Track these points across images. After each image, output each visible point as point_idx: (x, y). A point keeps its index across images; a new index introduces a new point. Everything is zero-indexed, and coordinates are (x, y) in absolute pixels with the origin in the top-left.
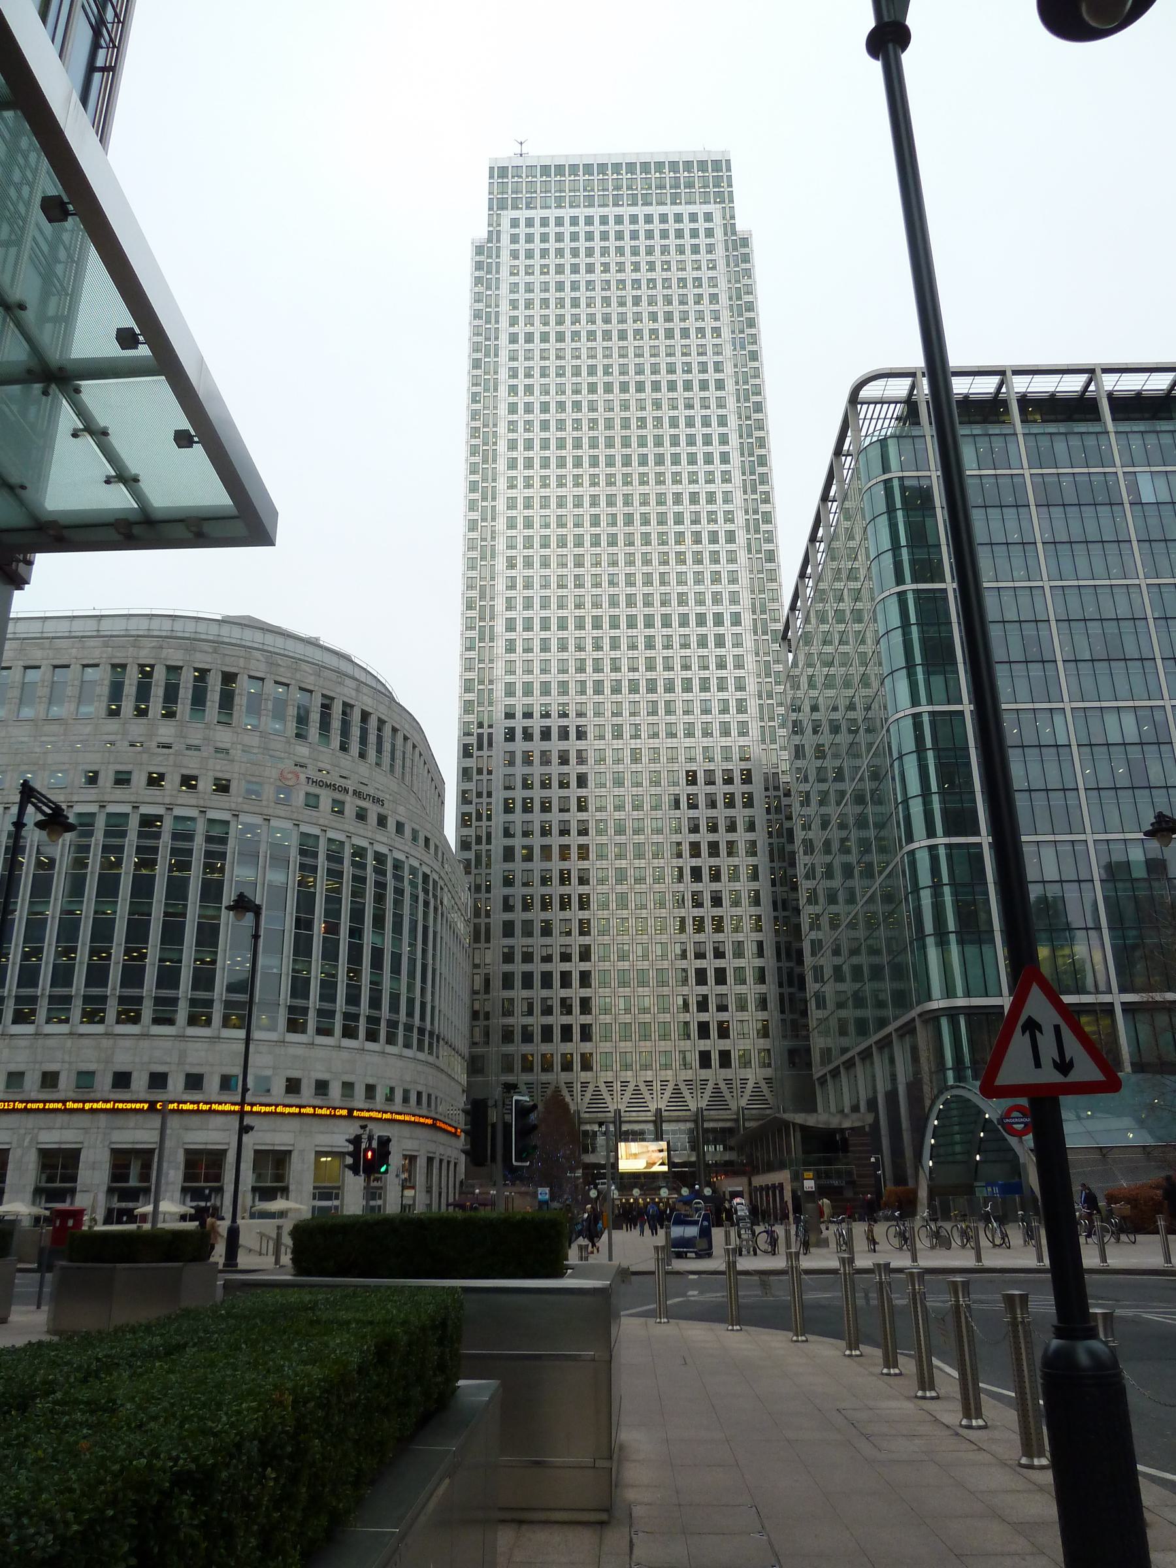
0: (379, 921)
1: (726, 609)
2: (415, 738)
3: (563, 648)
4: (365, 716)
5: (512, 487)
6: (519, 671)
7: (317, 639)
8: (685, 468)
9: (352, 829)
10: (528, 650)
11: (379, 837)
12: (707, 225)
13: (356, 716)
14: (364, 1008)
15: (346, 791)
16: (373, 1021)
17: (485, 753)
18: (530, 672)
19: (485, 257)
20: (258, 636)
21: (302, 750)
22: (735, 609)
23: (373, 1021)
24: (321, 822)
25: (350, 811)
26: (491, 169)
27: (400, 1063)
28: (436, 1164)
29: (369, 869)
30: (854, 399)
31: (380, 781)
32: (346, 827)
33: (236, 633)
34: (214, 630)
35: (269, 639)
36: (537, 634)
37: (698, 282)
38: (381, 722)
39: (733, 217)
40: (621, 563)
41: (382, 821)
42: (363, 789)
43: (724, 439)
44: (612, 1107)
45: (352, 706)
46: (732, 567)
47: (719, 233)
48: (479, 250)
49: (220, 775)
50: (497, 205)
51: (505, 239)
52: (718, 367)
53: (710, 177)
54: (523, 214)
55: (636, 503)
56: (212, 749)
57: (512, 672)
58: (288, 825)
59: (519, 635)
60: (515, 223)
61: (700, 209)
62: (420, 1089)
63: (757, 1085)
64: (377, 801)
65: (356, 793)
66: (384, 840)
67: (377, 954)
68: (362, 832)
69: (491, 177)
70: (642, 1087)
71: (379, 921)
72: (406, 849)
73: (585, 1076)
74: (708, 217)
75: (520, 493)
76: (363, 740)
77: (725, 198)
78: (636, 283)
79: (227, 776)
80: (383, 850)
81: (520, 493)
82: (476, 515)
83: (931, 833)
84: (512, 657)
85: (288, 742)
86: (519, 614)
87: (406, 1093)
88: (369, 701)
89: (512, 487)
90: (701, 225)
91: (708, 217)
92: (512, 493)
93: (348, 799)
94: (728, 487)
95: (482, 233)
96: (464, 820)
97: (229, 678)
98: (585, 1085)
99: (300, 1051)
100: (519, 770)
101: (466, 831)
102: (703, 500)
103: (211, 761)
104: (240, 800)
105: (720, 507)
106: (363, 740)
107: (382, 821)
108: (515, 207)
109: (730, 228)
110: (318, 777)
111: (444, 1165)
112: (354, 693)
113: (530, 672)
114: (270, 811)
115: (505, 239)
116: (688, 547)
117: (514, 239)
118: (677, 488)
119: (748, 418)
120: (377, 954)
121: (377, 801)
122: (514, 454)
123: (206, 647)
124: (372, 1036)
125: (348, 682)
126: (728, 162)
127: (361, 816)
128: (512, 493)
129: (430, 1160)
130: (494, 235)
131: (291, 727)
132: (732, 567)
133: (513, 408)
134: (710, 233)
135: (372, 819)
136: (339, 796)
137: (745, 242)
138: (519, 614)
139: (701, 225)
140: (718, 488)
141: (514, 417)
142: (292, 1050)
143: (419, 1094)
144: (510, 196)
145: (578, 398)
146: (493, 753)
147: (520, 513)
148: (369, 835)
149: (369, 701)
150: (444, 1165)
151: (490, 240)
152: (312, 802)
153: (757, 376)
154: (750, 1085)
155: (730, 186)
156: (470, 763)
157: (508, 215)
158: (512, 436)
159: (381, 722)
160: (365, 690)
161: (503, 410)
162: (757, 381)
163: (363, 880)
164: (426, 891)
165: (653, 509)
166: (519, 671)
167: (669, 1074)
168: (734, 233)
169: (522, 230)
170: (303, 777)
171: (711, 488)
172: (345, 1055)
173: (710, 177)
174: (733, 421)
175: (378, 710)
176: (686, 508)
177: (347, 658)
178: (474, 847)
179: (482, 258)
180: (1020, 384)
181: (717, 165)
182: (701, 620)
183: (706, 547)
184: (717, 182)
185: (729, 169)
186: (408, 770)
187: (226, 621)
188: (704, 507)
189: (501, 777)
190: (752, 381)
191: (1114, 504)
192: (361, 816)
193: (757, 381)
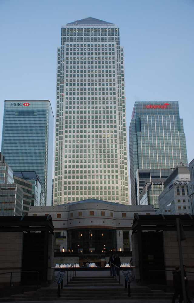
19: (60, 51)
26: (62, 29)
39: (119, 44)
47: (116, 50)
48: (59, 50)
51: (65, 50)
54: (70, 43)
60: (68, 45)
61: (111, 43)
90: (111, 47)
91: (113, 45)
92: (67, 115)
95: (60, 45)
126: (119, 29)
130: (62, 48)
151: (62, 49)
173: (114, 34)
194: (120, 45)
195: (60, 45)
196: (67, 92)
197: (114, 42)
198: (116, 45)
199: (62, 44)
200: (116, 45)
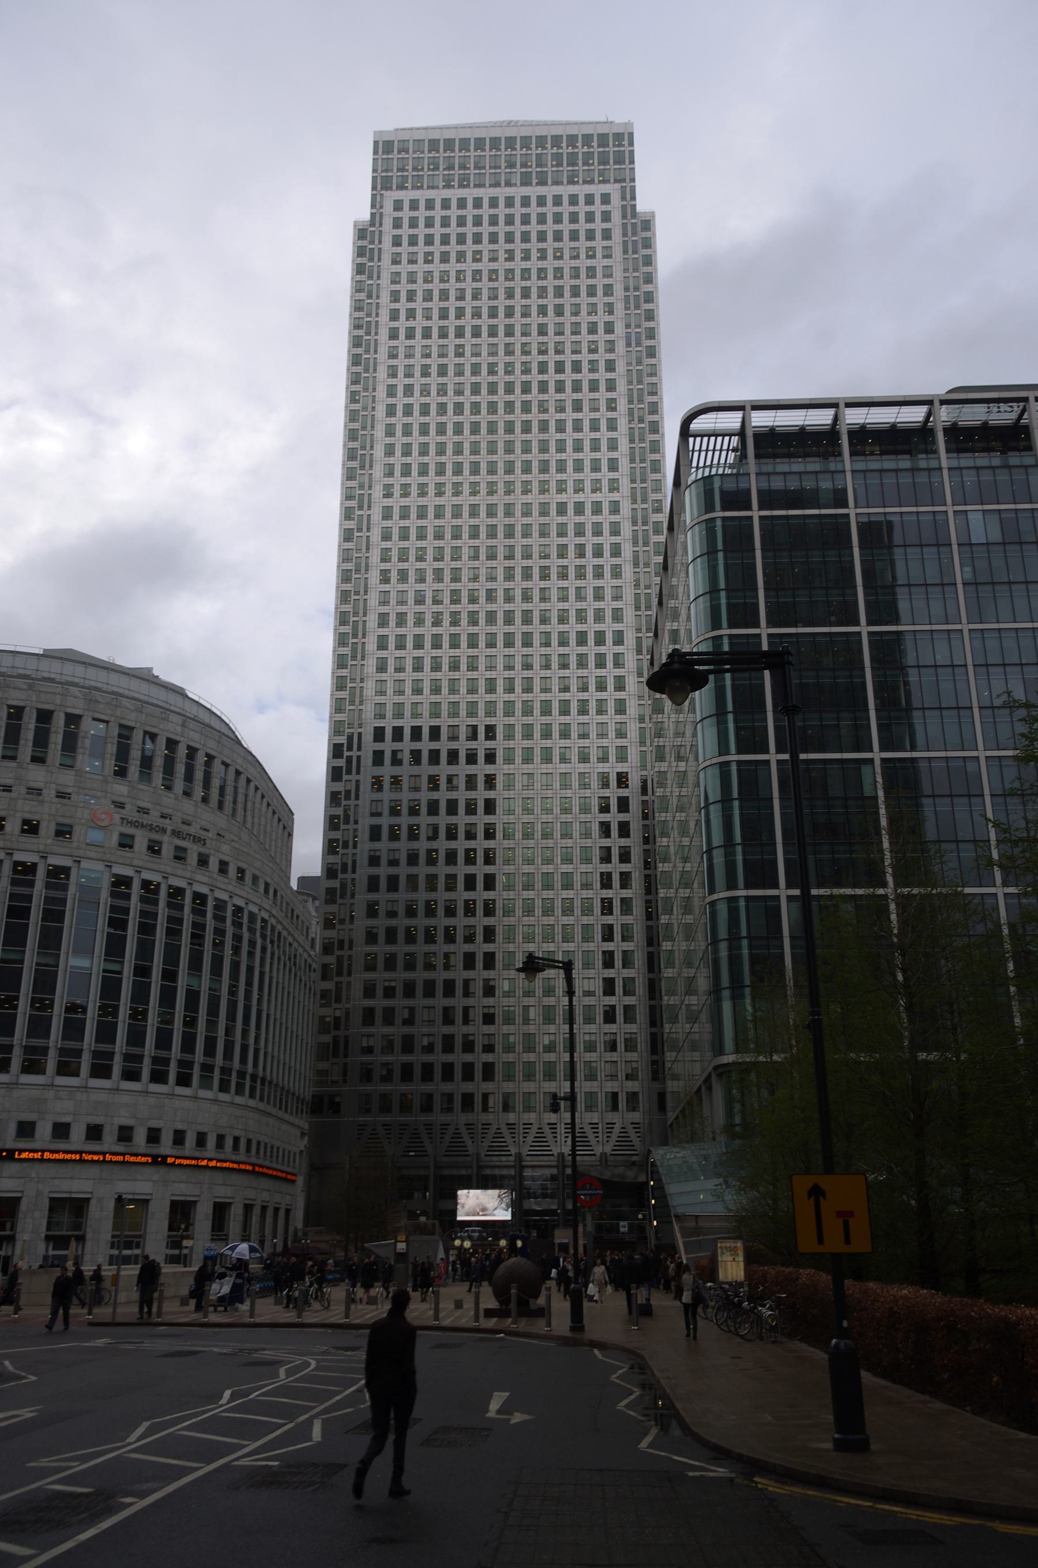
0: (195, 964)
1: (609, 627)
2: (252, 772)
3: (436, 667)
4: (192, 752)
5: (388, 495)
6: (390, 692)
7: (150, 670)
8: (570, 476)
9: (169, 870)
10: (399, 669)
11: (199, 877)
12: (604, 208)
13: (182, 752)
14: (176, 1051)
15: (164, 831)
16: (185, 1065)
18: (401, 693)
20: (80, 670)
21: (120, 789)
22: (618, 627)
23: (185, 1065)
24: (136, 862)
25: (167, 851)
26: (376, 143)
27: (215, 1108)
28: (256, 1211)
29: (187, 910)
30: (685, 432)
31: (208, 818)
32: (163, 868)
33: (53, 669)
34: (32, 664)
35: (92, 673)
36: (410, 653)
37: (591, 272)
38: (210, 758)
39: (633, 198)
41: (203, 861)
42: (185, 829)
43: (613, 446)
44: (471, 1149)
45: (176, 743)
49: (28, 816)
50: (381, 184)
51: (388, 223)
52: (610, 366)
53: (608, 152)
54: (406, 196)
55: (518, 513)
56: (24, 791)
57: (382, 693)
58: (100, 866)
59: (391, 654)
60: (398, 206)
61: (597, 190)
62: (237, 1133)
63: (624, 1130)
64: (197, 840)
65: (177, 834)
66: (205, 879)
67: (193, 997)
68: (180, 872)
69: (375, 152)
70: (505, 1130)
71: (195, 964)
72: (230, 888)
73: (443, 1118)
75: (396, 502)
76: (189, 777)
78: (526, 274)
79: (37, 817)
80: (204, 890)
81: (396, 502)
82: (351, 525)
83: (732, 885)
84: (383, 676)
85: (106, 781)
86: (391, 631)
87: (221, 1138)
88: (196, 736)
89: (388, 495)
91: (606, 199)
92: (388, 502)
93: (166, 839)
94: (615, 496)
95: (365, 214)
97: (45, 716)
98: (445, 1126)
99: (103, 1097)
100: (387, 795)
101: (333, 859)
102: (588, 511)
103: (20, 802)
104: (49, 841)
105: (606, 518)
106: (189, 777)
107: (203, 861)
108: (401, 187)
109: (629, 210)
110: (136, 816)
111: (270, 1213)
112: (179, 729)
113: (401, 693)
114: (81, 853)
115: (388, 223)
116: (571, 561)
117: (397, 224)
118: (562, 498)
119: (641, 420)
120: (193, 997)
121: (197, 840)
123: (20, 683)
124: (184, 1080)
125: (173, 718)
126: (631, 135)
127: (180, 855)
128: (388, 502)
129: (248, 1208)
130: (376, 218)
131: (110, 765)
133: (391, 411)
134: (606, 217)
135: (193, 859)
136: (156, 836)
137: (647, 224)
138: (391, 631)
139: (598, 208)
140: (605, 497)
142: (95, 1096)
143: (236, 1139)
144: (394, 173)
145: (461, 399)
146: (360, 777)
147: (395, 524)
148: (188, 875)
149: (196, 736)
150: (270, 1213)
151: (372, 223)
152: (126, 843)
153: (653, 374)
154: (617, 1129)
155: (632, 162)
157: (391, 196)
159: (210, 758)
160: (191, 724)
161: (380, 412)
162: (654, 380)
163: (180, 922)
164: (252, 930)
165: (535, 520)
166: (390, 692)
167: (532, 1117)
168: (634, 214)
169: (406, 214)
170: (117, 818)
172: (152, 1100)
173: (608, 152)
174: (623, 425)
175: (206, 745)
176: (571, 519)
177: (180, 692)
178: (340, 876)
179: (364, 243)
180: (854, 417)
181: (619, 137)
182: (582, 639)
183: (590, 561)
184: (619, 160)
185: (631, 143)
186: (240, 806)
187: (49, 655)
188: (589, 519)
189: (368, 803)
190: (648, 380)
191: (942, 544)
192: (180, 855)
193: (654, 380)
194: (640, 208)
195: (367, 217)
196: (391, 401)
197: (613, 189)
199: (373, 206)
200: (616, 200)
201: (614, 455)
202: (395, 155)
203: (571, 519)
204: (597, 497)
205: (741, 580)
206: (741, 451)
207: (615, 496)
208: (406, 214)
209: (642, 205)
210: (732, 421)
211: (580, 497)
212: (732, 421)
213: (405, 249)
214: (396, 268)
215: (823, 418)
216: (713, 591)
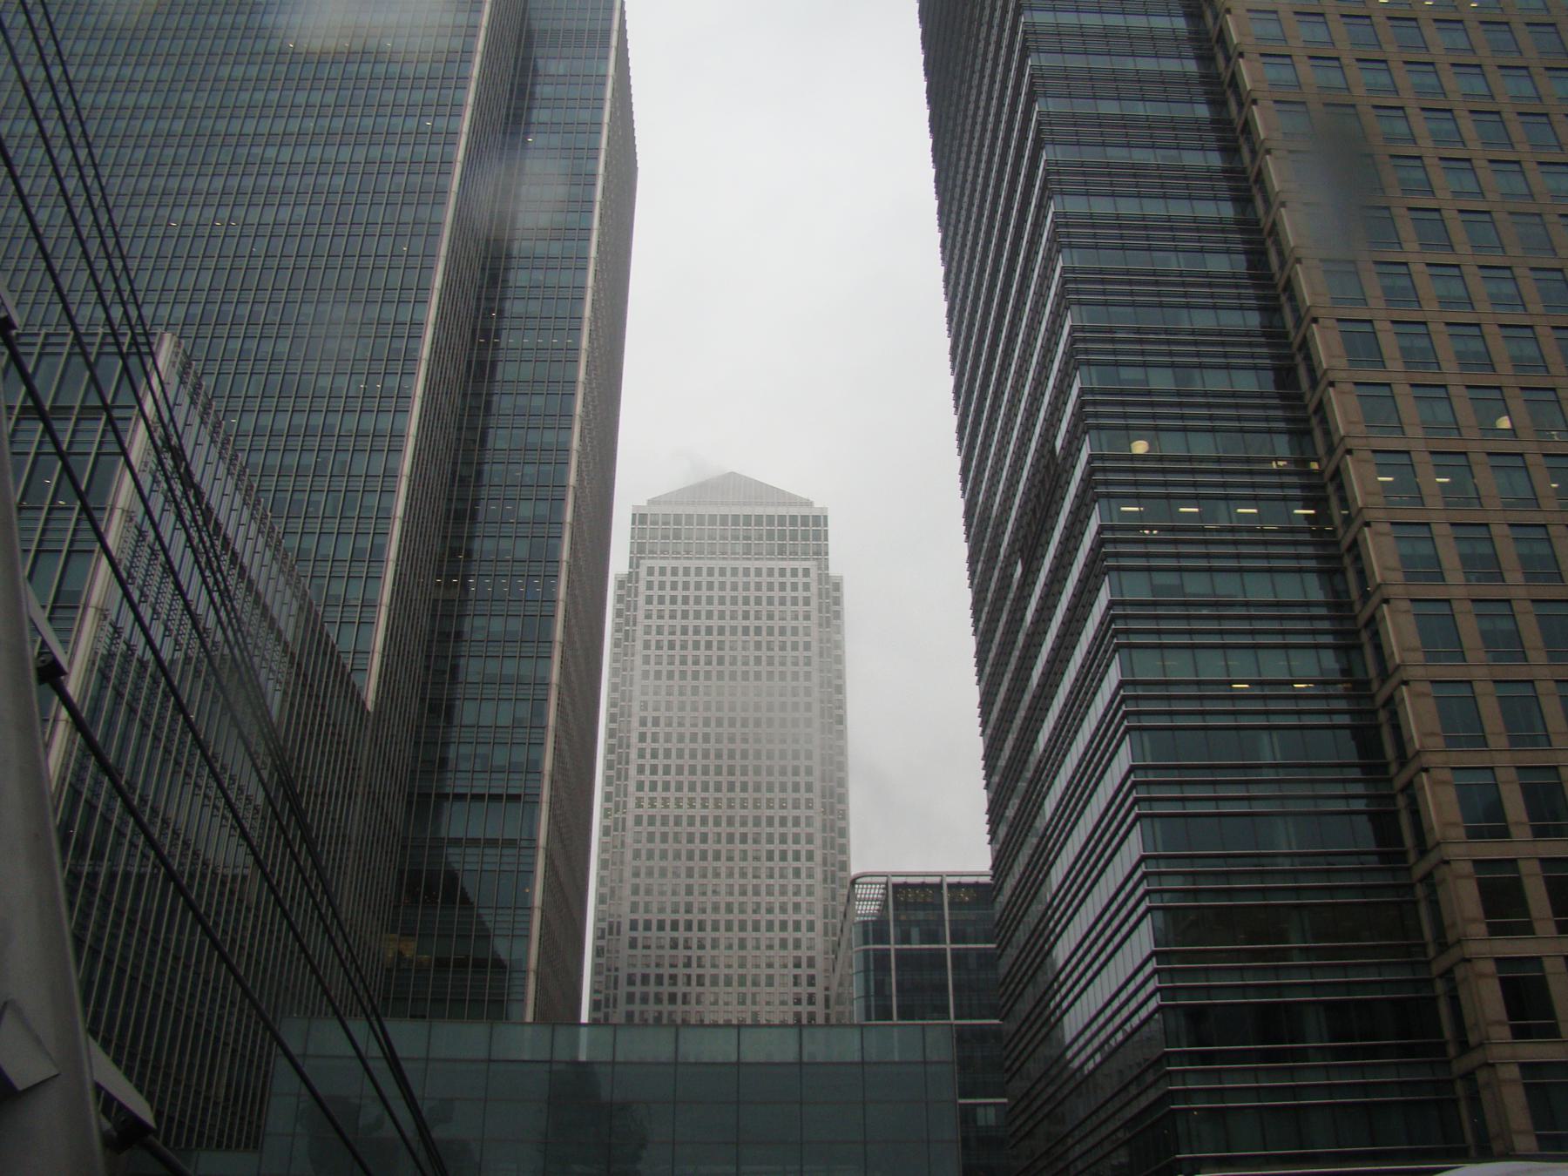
5: (639, 806)
17: (614, 937)
39: (827, 568)
40: (723, 875)
46: (809, 882)
60: (650, 571)
61: (800, 565)
74: (806, 572)
77: (821, 553)
90: (800, 579)
91: (806, 572)
94: (810, 813)
96: (595, 1005)
109: (824, 578)
117: (650, 586)
122: (642, 778)
128: (639, 811)
132: (809, 882)
134: (807, 587)
137: (837, 587)
139: (800, 579)
140: (802, 813)
141: (643, 745)
156: (603, 943)
158: (640, 761)
171: (796, 813)
184: (817, 537)
198: (814, 573)
200: (814, 573)
201: (810, 779)
202: (648, 526)
203: (777, 830)
204: (796, 813)
205: (881, 989)
206: (886, 889)
207: (810, 813)
208: (656, 578)
209: (834, 570)
210: (884, 879)
211: (784, 813)
212: (884, 879)
213: (655, 607)
214: (648, 622)
215: (936, 880)
216: (867, 996)
